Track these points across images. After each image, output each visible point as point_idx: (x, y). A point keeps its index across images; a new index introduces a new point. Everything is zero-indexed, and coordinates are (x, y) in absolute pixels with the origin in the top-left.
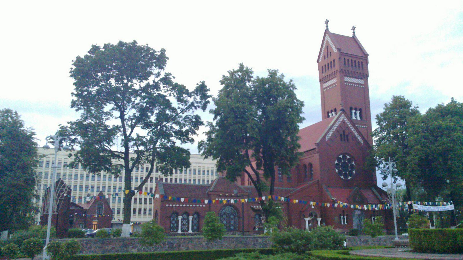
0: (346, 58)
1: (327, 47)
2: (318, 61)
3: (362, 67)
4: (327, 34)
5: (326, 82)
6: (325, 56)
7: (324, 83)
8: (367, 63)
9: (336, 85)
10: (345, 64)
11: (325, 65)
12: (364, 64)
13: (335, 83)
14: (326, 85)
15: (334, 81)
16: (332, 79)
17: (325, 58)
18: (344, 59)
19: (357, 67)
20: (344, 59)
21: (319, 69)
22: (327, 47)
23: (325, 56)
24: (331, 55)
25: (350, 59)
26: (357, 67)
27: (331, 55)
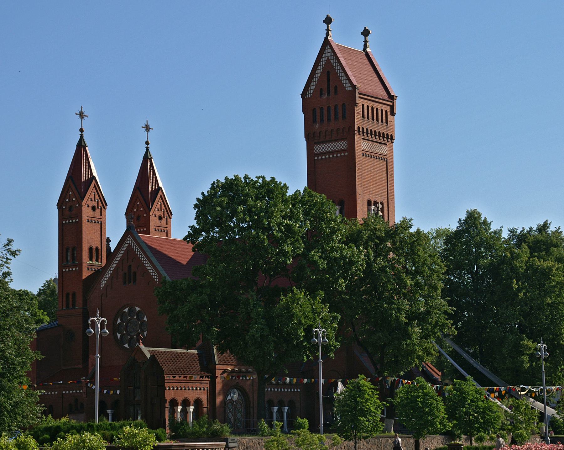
0: (366, 103)
1: (328, 72)
2: (303, 95)
3: (387, 122)
4: (328, 47)
5: (323, 143)
6: (321, 90)
7: (314, 143)
8: (393, 114)
9: (346, 154)
10: (363, 116)
11: (321, 109)
12: (389, 117)
13: (344, 151)
14: (319, 148)
15: (342, 145)
16: (336, 140)
17: (321, 94)
18: (363, 105)
19: (380, 121)
20: (363, 105)
21: (304, 111)
22: (328, 72)
23: (321, 90)
24: (336, 92)
25: (370, 104)
26: (380, 121)
27: (336, 92)
